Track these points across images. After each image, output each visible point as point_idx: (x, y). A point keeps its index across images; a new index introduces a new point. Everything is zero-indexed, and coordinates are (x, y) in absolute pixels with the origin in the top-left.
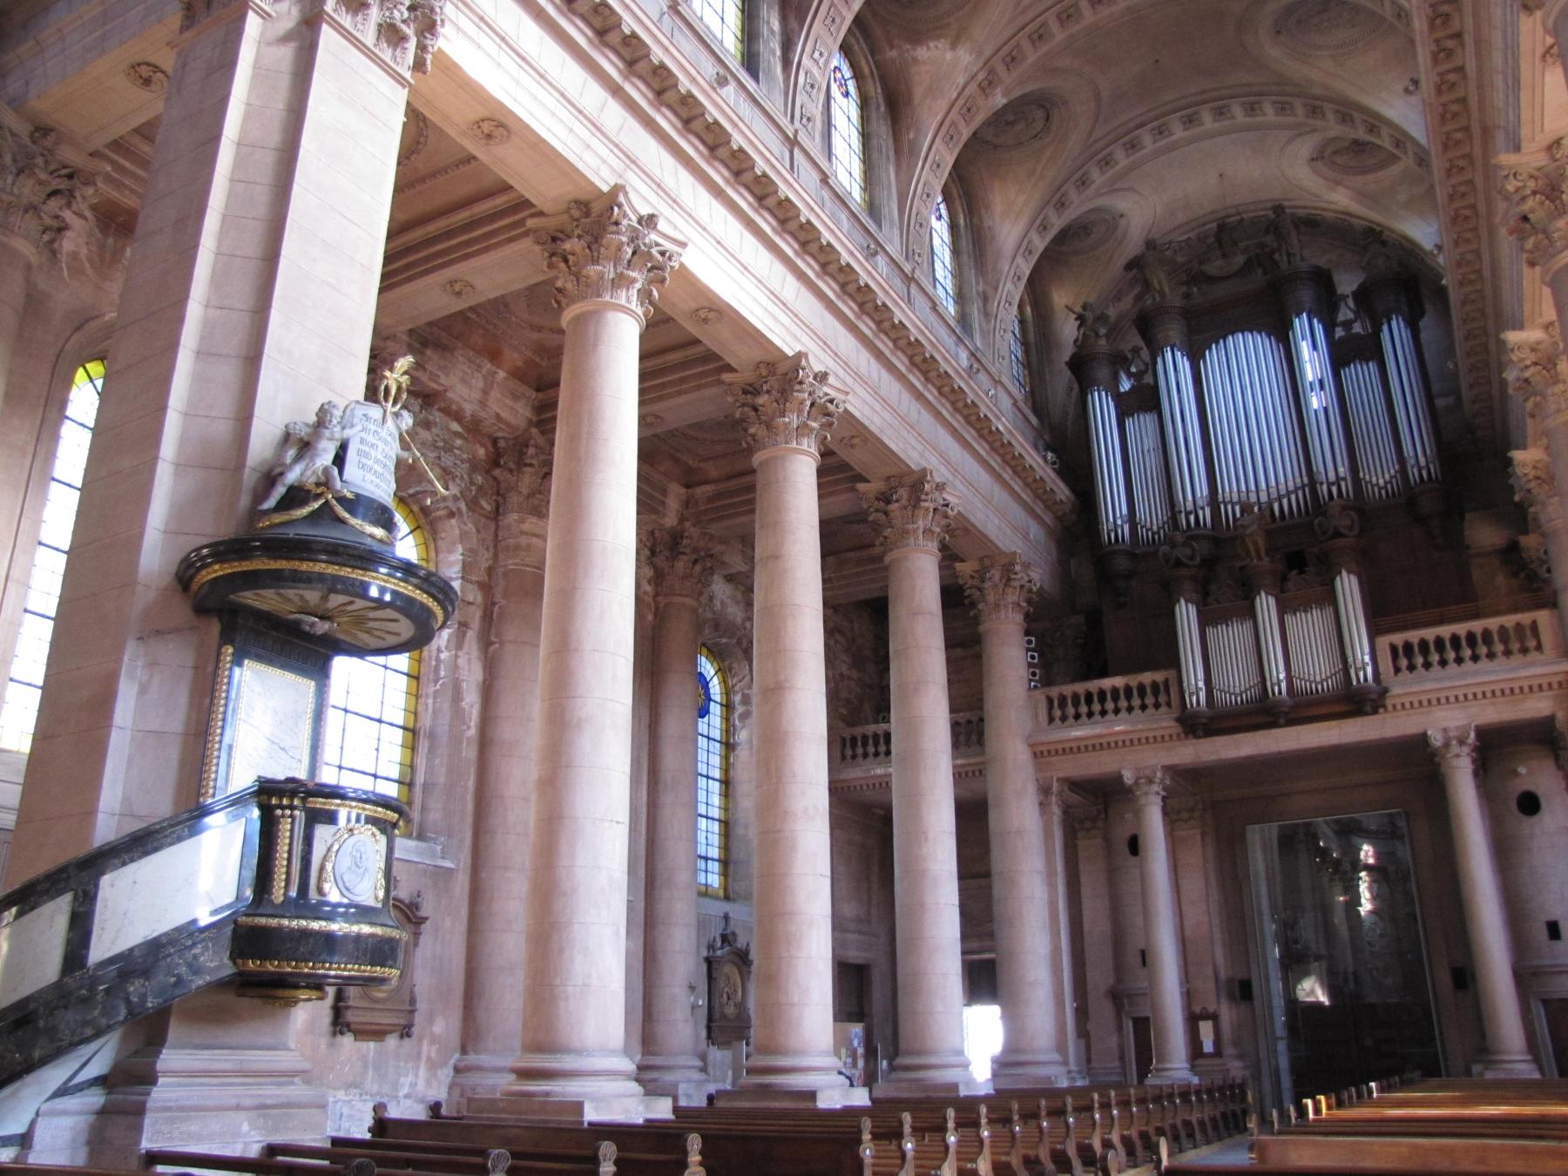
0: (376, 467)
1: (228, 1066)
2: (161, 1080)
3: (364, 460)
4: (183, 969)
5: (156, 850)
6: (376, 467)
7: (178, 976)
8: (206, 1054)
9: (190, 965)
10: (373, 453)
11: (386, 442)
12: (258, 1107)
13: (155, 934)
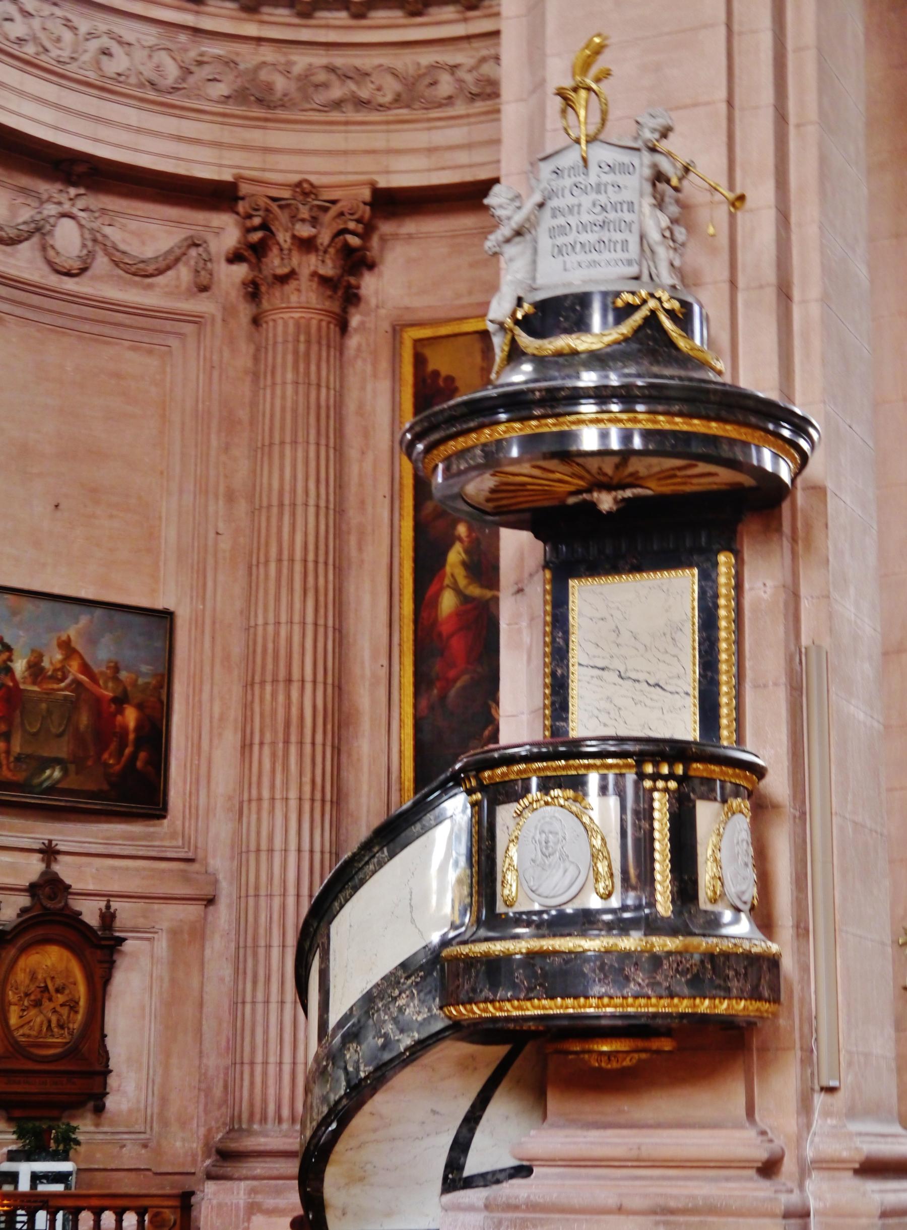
0: (584, 237)
1: (619, 1152)
2: (535, 1169)
3: (560, 240)
4: (389, 1028)
5: (362, 882)
6: (584, 237)
7: (386, 1036)
8: (594, 1135)
9: (395, 1020)
10: (573, 221)
11: (599, 188)
12: (653, 1212)
13: (369, 987)
